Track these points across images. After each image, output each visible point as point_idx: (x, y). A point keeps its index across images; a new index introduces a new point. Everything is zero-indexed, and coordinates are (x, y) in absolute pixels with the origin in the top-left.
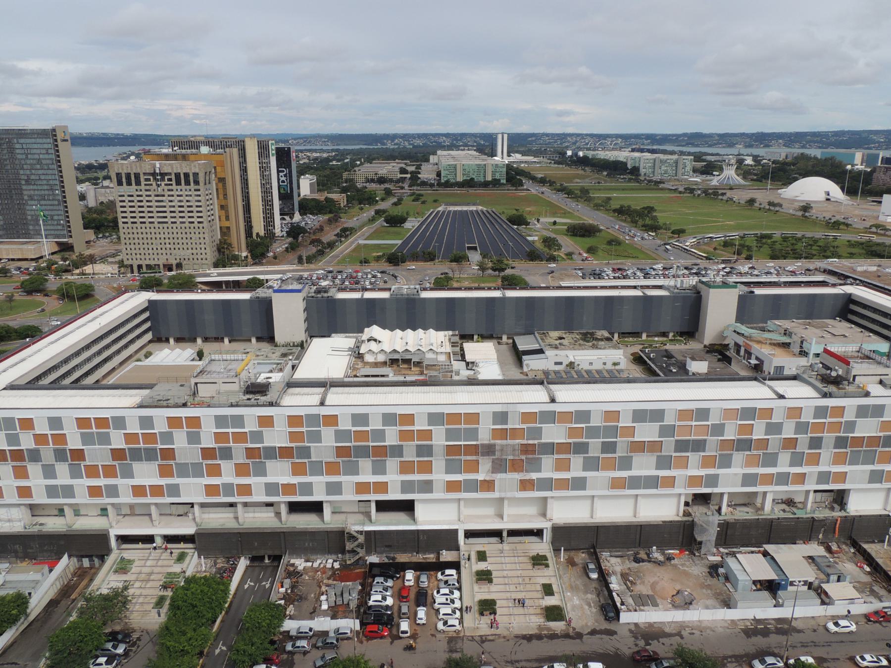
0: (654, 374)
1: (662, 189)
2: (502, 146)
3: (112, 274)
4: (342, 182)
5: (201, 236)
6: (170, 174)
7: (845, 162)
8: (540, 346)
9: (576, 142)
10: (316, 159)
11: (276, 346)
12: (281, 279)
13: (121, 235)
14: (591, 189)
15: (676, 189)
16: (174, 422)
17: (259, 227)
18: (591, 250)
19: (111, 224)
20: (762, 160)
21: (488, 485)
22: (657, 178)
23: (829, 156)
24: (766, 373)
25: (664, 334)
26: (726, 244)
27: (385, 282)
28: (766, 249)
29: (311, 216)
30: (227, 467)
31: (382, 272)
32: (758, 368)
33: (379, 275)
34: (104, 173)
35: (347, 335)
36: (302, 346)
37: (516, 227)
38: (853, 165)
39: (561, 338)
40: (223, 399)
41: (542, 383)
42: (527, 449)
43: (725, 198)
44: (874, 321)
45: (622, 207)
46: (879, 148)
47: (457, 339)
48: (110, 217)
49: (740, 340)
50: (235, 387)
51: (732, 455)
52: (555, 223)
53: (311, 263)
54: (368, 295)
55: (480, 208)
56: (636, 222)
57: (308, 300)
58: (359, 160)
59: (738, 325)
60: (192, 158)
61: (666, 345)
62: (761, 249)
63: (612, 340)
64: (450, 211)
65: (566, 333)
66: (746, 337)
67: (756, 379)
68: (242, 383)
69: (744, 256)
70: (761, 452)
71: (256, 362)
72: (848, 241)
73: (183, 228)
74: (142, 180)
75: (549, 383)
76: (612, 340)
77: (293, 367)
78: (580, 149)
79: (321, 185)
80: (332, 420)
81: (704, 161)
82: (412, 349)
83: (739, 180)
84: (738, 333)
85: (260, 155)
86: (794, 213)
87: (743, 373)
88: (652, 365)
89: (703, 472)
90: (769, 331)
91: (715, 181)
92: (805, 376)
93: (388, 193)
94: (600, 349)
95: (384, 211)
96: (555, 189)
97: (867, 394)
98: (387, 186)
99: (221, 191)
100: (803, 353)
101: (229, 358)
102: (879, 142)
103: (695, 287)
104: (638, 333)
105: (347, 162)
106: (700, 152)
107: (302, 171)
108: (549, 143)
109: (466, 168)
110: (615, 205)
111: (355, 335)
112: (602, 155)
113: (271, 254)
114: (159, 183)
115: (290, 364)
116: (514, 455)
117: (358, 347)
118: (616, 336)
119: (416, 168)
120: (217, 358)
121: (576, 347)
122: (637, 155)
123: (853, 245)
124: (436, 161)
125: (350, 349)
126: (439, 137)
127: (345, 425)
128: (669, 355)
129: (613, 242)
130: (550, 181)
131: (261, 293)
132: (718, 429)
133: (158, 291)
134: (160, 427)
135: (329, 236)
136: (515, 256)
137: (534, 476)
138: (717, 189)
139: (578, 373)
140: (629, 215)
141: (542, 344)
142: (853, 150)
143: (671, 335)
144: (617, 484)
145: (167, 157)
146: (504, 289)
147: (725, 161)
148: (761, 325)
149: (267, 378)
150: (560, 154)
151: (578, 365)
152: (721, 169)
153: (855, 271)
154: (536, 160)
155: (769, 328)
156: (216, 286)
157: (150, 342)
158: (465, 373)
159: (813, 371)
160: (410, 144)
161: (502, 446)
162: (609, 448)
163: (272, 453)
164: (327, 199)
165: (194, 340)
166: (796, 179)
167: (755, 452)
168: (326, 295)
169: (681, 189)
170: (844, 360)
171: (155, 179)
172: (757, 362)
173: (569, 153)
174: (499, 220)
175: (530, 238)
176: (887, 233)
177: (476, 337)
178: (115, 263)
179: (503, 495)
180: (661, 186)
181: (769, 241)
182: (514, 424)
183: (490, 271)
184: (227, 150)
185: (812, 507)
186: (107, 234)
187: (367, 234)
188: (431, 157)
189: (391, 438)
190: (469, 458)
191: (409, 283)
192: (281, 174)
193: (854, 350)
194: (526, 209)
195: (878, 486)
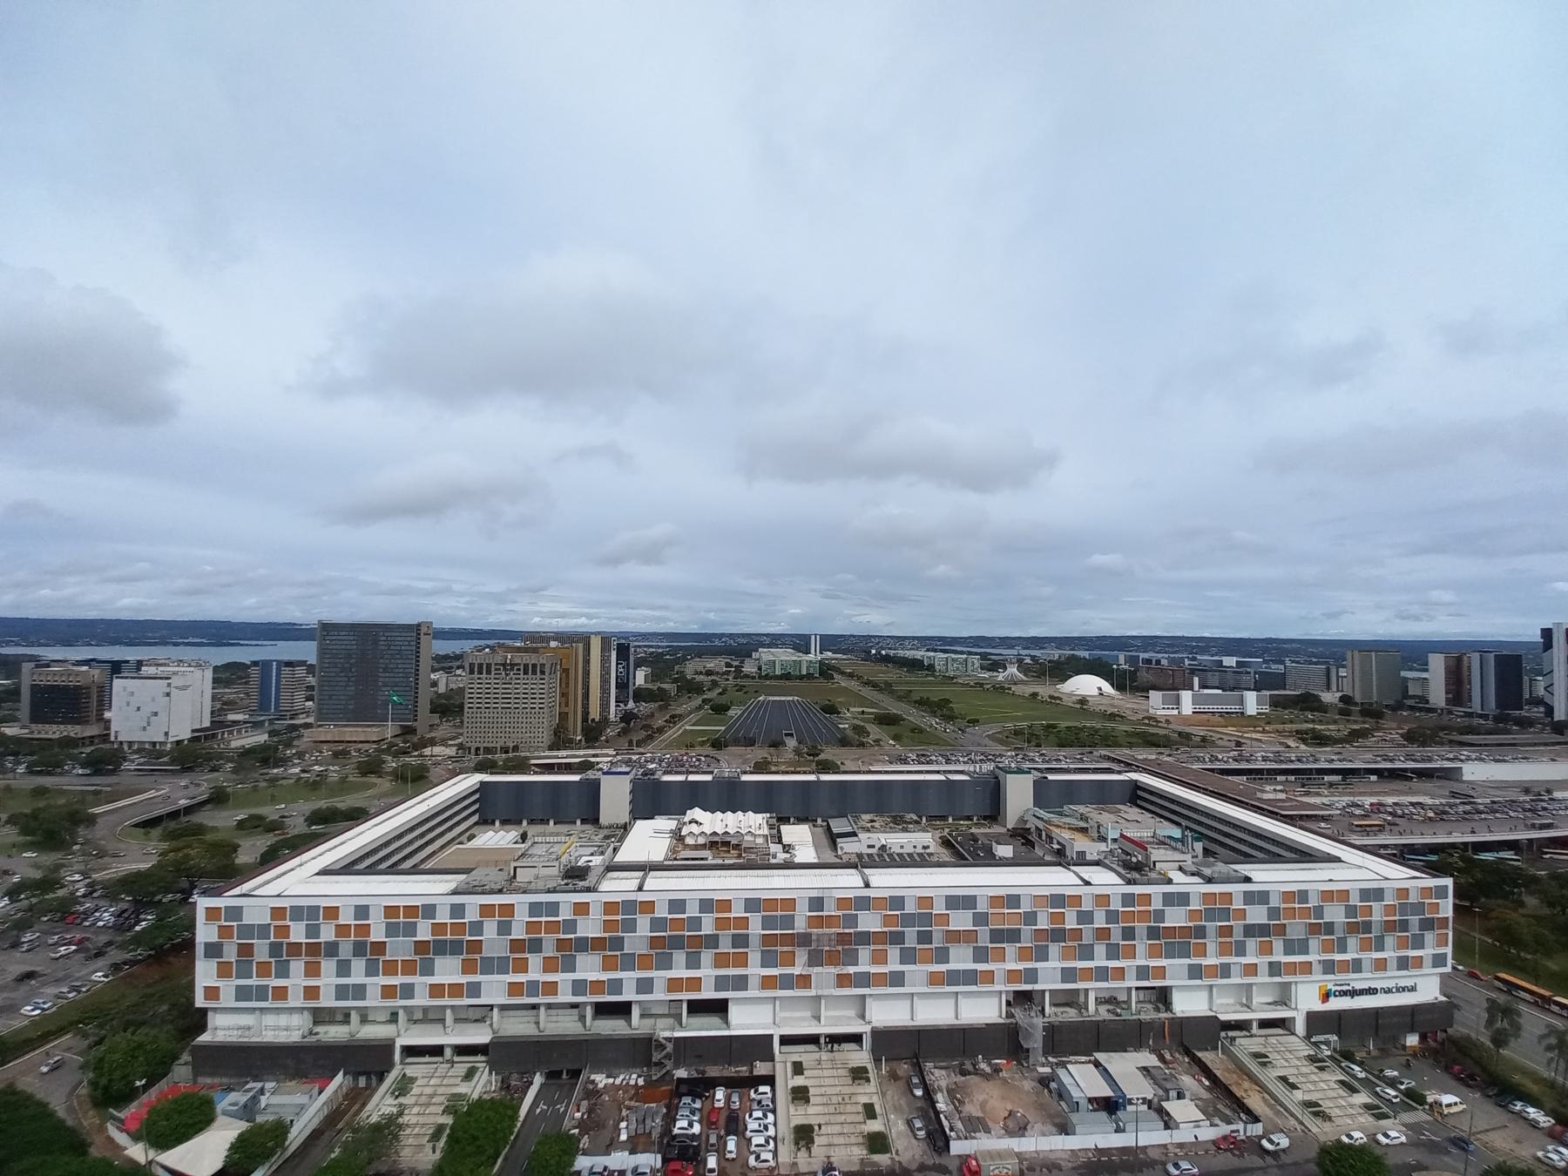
2: (814, 645)
6: (519, 664)
10: (652, 653)
11: (600, 828)
12: (611, 762)
13: (466, 720)
16: (486, 910)
17: (595, 714)
18: (896, 738)
21: (804, 981)
22: (952, 674)
23: (1097, 657)
24: (1070, 858)
25: (969, 818)
26: (1017, 733)
28: (1052, 737)
29: (644, 704)
30: (535, 961)
31: (706, 756)
32: (1061, 853)
33: (703, 759)
34: (458, 663)
36: (626, 828)
38: (1118, 665)
39: (873, 821)
40: (540, 885)
41: (856, 867)
42: (843, 939)
47: (774, 821)
48: (457, 703)
49: (1041, 825)
50: (554, 871)
51: (1047, 946)
52: (863, 712)
54: (692, 778)
55: (796, 698)
66: (1045, 821)
67: (1060, 864)
71: (578, 844)
72: (1126, 731)
74: (493, 669)
75: (862, 867)
77: (615, 849)
80: (648, 907)
81: (989, 659)
82: (732, 832)
84: (1038, 818)
85: (603, 650)
86: (1073, 705)
87: (1048, 858)
88: (960, 849)
89: (1021, 966)
92: (1106, 861)
93: (715, 684)
94: (910, 832)
95: (710, 700)
97: (1170, 882)
98: (713, 677)
100: (1103, 839)
101: (552, 841)
106: (985, 652)
107: (638, 664)
112: (901, 653)
113: (604, 738)
115: (612, 846)
117: (679, 829)
118: (924, 819)
120: (540, 841)
121: (888, 830)
125: (671, 831)
127: (662, 912)
128: (975, 839)
131: (591, 775)
132: (1031, 918)
133: (491, 773)
134: (472, 916)
135: (659, 722)
137: (851, 970)
139: (890, 855)
141: (855, 827)
142: (1116, 652)
143: (975, 819)
144: (935, 979)
145: (519, 650)
146: (819, 773)
150: (865, 652)
151: (890, 848)
152: (1005, 668)
153: (1136, 760)
154: (844, 657)
156: (549, 768)
157: (476, 824)
158: (781, 857)
159: (1113, 857)
161: (818, 935)
162: (925, 937)
163: (584, 945)
165: (520, 823)
166: (1072, 677)
167: (1070, 944)
168: (652, 777)
169: (972, 684)
170: (1141, 845)
171: (505, 669)
172: (1058, 847)
173: (874, 652)
175: (841, 726)
176: (1159, 724)
177: (792, 820)
178: (454, 745)
179: (820, 993)
182: (830, 910)
184: (574, 645)
185: (1136, 1007)
188: (754, 654)
189: (707, 928)
190: (785, 949)
192: (620, 666)
195: (1198, 982)
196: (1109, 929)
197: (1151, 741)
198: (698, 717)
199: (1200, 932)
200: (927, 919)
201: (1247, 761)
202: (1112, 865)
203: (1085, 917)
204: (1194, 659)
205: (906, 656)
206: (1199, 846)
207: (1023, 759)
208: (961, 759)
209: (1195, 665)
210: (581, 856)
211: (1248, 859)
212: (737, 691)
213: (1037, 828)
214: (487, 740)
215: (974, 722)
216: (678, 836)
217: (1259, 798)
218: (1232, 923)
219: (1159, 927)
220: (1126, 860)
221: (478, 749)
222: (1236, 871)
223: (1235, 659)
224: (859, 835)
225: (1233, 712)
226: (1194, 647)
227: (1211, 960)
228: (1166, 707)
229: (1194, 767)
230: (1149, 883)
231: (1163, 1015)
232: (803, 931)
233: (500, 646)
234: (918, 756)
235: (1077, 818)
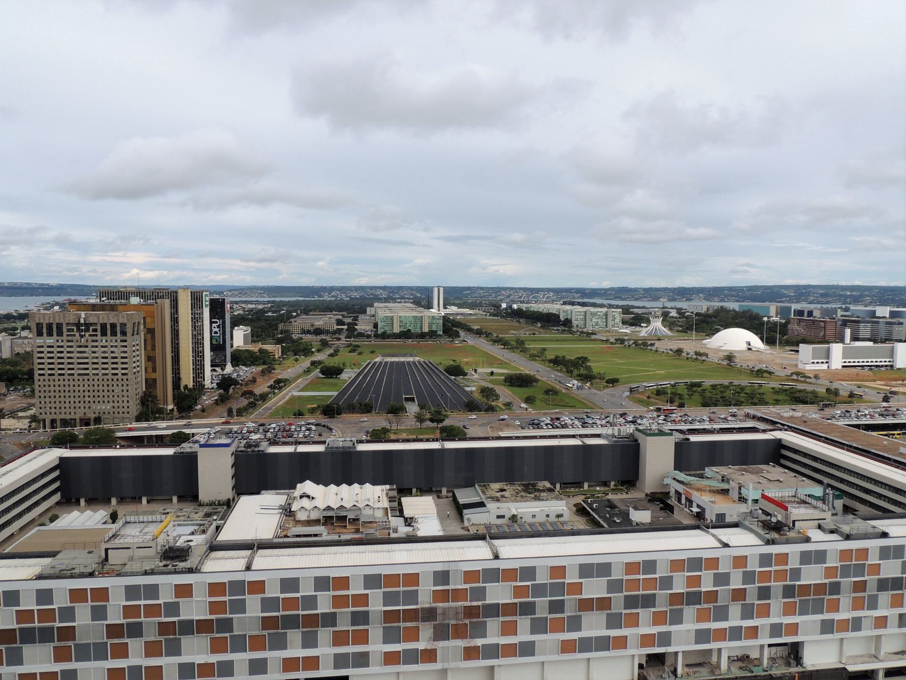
0: (598, 525)
1: (594, 340)
2: (437, 298)
3: (21, 429)
4: (278, 334)
5: (125, 388)
6: (96, 324)
7: (762, 314)
8: (481, 498)
9: (510, 295)
10: (251, 310)
11: (200, 505)
13: (36, 387)
14: (526, 340)
15: (607, 341)
16: (77, 595)
17: (187, 379)
18: (529, 400)
19: (26, 377)
20: (685, 313)
21: (429, 656)
22: (589, 329)
24: (709, 521)
25: (605, 484)
26: (659, 393)
27: (320, 435)
28: (697, 397)
29: (244, 368)
30: (135, 645)
31: (317, 425)
32: (700, 516)
33: (314, 428)
34: (24, 323)
35: (278, 491)
36: (229, 505)
37: (453, 377)
38: (769, 317)
39: (502, 490)
40: (136, 566)
41: (483, 538)
42: (471, 612)
43: (654, 348)
44: (805, 465)
45: (557, 357)
46: (790, 301)
47: (394, 493)
48: (25, 369)
49: (681, 488)
51: (682, 609)
52: (492, 373)
53: (242, 416)
54: (302, 449)
55: (417, 358)
56: (571, 372)
57: (237, 455)
58: (296, 311)
59: (677, 472)
60: (120, 308)
61: (608, 494)
62: (693, 397)
63: (554, 491)
64: (386, 363)
65: (507, 485)
68: (159, 548)
69: (676, 403)
70: (711, 606)
71: (176, 523)
72: (773, 388)
73: (105, 380)
74: (65, 330)
75: (492, 538)
76: (554, 491)
78: (515, 302)
79: (256, 336)
80: (258, 587)
81: (632, 313)
82: (348, 505)
83: (666, 331)
84: (678, 481)
87: (686, 521)
88: (596, 516)
89: (655, 630)
90: (707, 477)
91: (644, 332)
92: (747, 523)
93: (324, 344)
94: (543, 500)
95: (320, 362)
96: (491, 340)
97: (807, 540)
98: (323, 337)
99: (149, 342)
100: (742, 499)
101: (146, 520)
102: (789, 296)
103: (632, 435)
104: (580, 483)
105: (283, 314)
108: (485, 296)
109: (403, 319)
110: (551, 356)
111: (286, 491)
112: (535, 307)
113: (199, 407)
114: (83, 333)
116: (457, 619)
117: (289, 504)
118: (558, 486)
119: (353, 320)
120: (132, 520)
121: (518, 499)
122: (568, 307)
123: (777, 392)
124: (373, 313)
125: (281, 507)
126: (376, 290)
127: (273, 592)
128: (612, 505)
129: (550, 392)
130: (486, 333)
131: (186, 447)
132: (667, 582)
133: (71, 448)
134: (60, 601)
136: (453, 408)
137: (479, 642)
138: (646, 340)
140: (565, 366)
142: (767, 304)
143: (613, 483)
144: (567, 647)
145: (94, 307)
146: (443, 440)
147: (651, 313)
148: (698, 472)
149: (188, 541)
150: (495, 306)
151: (521, 518)
153: (782, 417)
154: (471, 312)
155: (707, 475)
156: (138, 442)
157: (58, 503)
158: (403, 530)
159: (753, 518)
160: (347, 297)
161: (444, 609)
162: (558, 607)
163: (188, 628)
164: (261, 350)
165: (108, 501)
166: (718, 331)
167: (706, 606)
168: (256, 449)
169: (612, 340)
170: (781, 505)
171: (79, 330)
172: (699, 510)
173: (504, 306)
174: (436, 371)
175: (467, 389)
176: (808, 380)
177: (414, 490)
178: (26, 417)
179: (446, 666)
180: (593, 337)
181: (699, 389)
182: (457, 584)
183: (428, 423)
184: (159, 301)
185: (768, 663)
186: (20, 387)
187: (302, 386)
188: (368, 309)
189: (324, 606)
190: (408, 624)
191: (344, 435)
192: (214, 325)
193: (790, 495)
194: (463, 360)
196: (745, 589)
197: (798, 398)
198: (307, 382)
199: (835, 588)
200: (559, 588)
201: (894, 415)
202: (751, 526)
203: (722, 579)
204: (847, 310)
205: (541, 310)
206: (839, 503)
207: (664, 420)
208: (599, 422)
209: (848, 316)
210: (180, 536)
211: (887, 514)
212: (350, 352)
213: (677, 492)
214: (63, 411)
215: (613, 382)
216: (288, 512)
217: (901, 453)
218: (866, 578)
219: (795, 585)
220: (766, 521)
221: (53, 422)
222: (874, 527)
223: (888, 309)
224: (488, 505)
225: (883, 366)
226: (846, 297)
227: (844, 614)
228: (815, 361)
229: (840, 423)
230: (788, 542)
231: (794, 670)
232: (429, 606)
233: (72, 303)
234: (552, 419)
235: (718, 480)
